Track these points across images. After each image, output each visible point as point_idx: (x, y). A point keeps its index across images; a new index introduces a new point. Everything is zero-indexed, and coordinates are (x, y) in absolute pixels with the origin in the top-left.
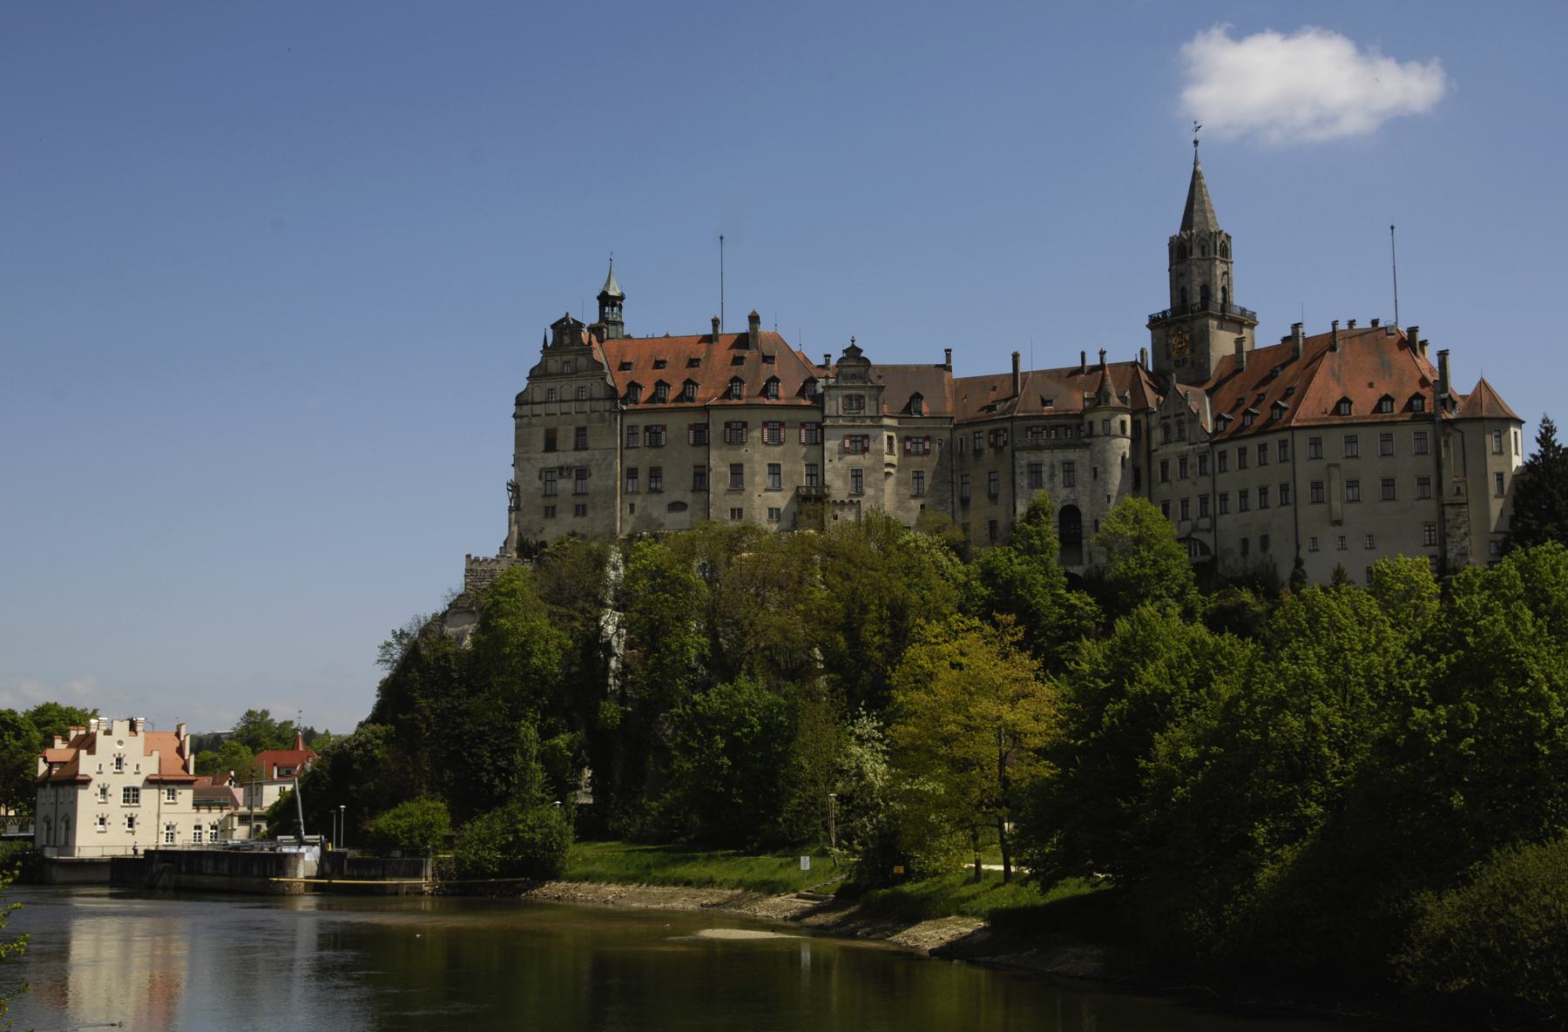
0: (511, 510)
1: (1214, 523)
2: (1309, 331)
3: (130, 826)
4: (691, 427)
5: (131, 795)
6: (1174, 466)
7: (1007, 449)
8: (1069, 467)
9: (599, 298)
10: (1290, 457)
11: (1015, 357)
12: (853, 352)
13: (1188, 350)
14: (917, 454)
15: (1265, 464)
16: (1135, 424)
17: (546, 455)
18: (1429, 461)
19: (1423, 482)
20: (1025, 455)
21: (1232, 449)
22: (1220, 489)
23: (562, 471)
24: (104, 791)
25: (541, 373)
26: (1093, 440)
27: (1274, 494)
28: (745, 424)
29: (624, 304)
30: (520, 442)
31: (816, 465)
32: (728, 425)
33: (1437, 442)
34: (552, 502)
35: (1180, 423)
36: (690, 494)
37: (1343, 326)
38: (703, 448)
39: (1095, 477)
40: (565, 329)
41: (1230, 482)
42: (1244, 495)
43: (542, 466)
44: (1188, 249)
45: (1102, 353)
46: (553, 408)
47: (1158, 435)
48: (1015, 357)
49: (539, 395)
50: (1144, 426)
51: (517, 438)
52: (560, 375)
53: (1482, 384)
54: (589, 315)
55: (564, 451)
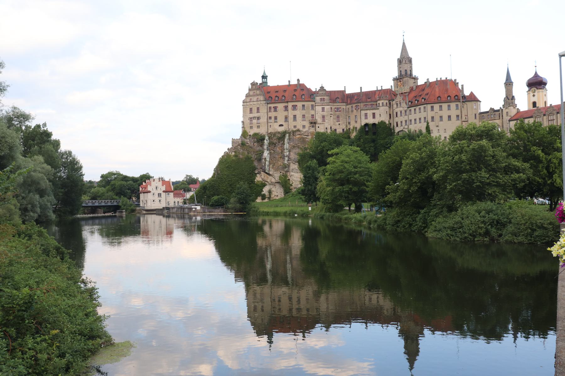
0: (242, 127)
2: (431, 81)
3: (160, 202)
4: (284, 107)
5: (159, 195)
7: (359, 110)
8: (374, 114)
10: (426, 110)
11: (361, 88)
12: (322, 88)
16: (390, 103)
19: (458, 116)
20: (363, 111)
21: (412, 109)
24: (154, 194)
27: (423, 120)
28: (297, 106)
29: (268, 78)
32: (292, 106)
33: (461, 106)
34: (251, 125)
35: (400, 103)
39: (380, 116)
40: (253, 84)
41: (412, 117)
42: (415, 120)
45: (382, 86)
46: (251, 103)
47: (395, 106)
48: (361, 88)
49: (248, 100)
50: (392, 104)
51: (243, 110)
53: (472, 94)
54: (259, 81)
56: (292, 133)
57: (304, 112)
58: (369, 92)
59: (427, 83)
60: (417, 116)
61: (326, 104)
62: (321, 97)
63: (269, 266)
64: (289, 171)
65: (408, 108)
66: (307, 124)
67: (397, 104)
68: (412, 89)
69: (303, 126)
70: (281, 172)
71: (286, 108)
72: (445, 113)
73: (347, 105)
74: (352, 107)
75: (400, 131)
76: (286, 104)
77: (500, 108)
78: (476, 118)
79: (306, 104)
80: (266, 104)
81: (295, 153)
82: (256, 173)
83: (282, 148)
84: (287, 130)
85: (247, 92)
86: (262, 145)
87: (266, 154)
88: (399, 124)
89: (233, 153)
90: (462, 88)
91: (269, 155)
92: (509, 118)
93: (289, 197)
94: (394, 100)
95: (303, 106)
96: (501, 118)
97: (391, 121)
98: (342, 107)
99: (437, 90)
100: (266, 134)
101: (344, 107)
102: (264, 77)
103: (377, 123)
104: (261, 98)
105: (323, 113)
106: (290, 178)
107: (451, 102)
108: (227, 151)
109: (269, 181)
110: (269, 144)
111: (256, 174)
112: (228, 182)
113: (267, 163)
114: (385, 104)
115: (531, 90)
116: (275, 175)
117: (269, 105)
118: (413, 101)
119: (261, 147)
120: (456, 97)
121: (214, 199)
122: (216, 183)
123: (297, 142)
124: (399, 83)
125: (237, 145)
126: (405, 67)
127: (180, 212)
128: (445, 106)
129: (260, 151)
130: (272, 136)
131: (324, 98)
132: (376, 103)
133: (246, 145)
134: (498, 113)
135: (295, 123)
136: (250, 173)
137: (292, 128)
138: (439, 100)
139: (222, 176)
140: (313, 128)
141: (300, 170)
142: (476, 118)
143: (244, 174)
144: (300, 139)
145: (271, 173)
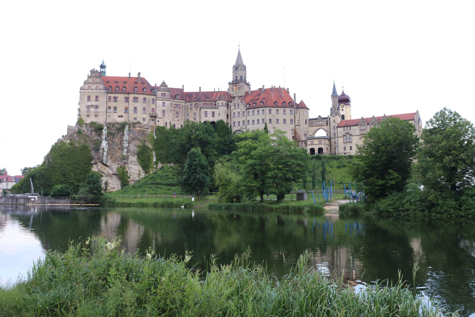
0: (78, 115)
1: (246, 127)
2: (266, 87)
4: (124, 98)
6: (237, 114)
7: (199, 108)
8: (213, 113)
9: (100, 66)
10: (265, 113)
11: (200, 88)
12: (164, 83)
13: (237, 90)
14: (177, 108)
15: (254, 115)
16: (228, 104)
17: (88, 102)
19: (291, 120)
20: (204, 109)
21: (251, 111)
22: (248, 120)
25: (87, 82)
27: (261, 121)
28: (138, 98)
29: (106, 68)
30: (81, 98)
31: (154, 109)
32: (134, 98)
34: (88, 114)
35: (238, 105)
37: (273, 87)
39: (219, 116)
41: (250, 118)
43: (86, 105)
46: (90, 91)
48: (200, 88)
49: (86, 87)
50: (229, 105)
52: (93, 83)
53: (302, 102)
54: (99, 69)
56: (132, 124)
57: (145, 105)
58: (207, 92)
59: (263, 89)
60: (256, 117)
61: (167, 99)
62: (162, 92)
64: (127, 163)
65: (246, 109)
66: (147, 117)
67: (235, 105)
68: (247, 93)
69: (143, 118)
70: (119, 164)
71: (127, 99)
72: (281, 116)
73: (186, 102)
75: (237, 130)
76: (127, 96)
77: (328, 116)
78: (306, 123)
79: (147, 97)
80: (105, 93)
81: (135, 145)
82: (93, 163)
84: (127, 121)
85: (86, 78)
86: (100, 135)
87: (104, 144)
88: (237, 124)
89: (68, 141)
90: (295, 97)
91: (107, 146)
92: (336, 125)
93: (130, 190)
94: (232, 102)
95: (145, 99)
96: (329, 124)
97: (229, 121)
98: (182, 104)
99: (273, 96)
100: (105, 124)
101: (184, 104)
102: (102, 67)
103: (216, 121)
104: (101, 86)
105: (163, 107)
106: (128, 170)
107: (286, 107)
108: (62, 138)
109: (105, 172)
110: (107, 134)
111: (92, 164)
112: (61, 172)
113: (105, 154)
114: (224, 104)
115: (340, 105)
116: (113, 166)
117: (109, 95)
118: (251, 103)
119: (99, 136)
120: (290, 104)
121: (56, 188)
122: (47, 172)
123: (137, 134)
124: (235, 87)
125: (73, 132)
126: (240, 73)
127: (11, 203)
128: (281, 110)
129: (98, 140)
130: (111, 126)
132: (215, 103)
133: (82, 134)
134: (326, 120)
135: (135, 116)
136: (87, 163)
137: (132, 120)
138: (275, 105)
139: (54, 164)
140: (153, 122)
141: (139, 162)
142: (306, 123)
143: (80, 164)
144: (140, 131)
145: (108, 164)
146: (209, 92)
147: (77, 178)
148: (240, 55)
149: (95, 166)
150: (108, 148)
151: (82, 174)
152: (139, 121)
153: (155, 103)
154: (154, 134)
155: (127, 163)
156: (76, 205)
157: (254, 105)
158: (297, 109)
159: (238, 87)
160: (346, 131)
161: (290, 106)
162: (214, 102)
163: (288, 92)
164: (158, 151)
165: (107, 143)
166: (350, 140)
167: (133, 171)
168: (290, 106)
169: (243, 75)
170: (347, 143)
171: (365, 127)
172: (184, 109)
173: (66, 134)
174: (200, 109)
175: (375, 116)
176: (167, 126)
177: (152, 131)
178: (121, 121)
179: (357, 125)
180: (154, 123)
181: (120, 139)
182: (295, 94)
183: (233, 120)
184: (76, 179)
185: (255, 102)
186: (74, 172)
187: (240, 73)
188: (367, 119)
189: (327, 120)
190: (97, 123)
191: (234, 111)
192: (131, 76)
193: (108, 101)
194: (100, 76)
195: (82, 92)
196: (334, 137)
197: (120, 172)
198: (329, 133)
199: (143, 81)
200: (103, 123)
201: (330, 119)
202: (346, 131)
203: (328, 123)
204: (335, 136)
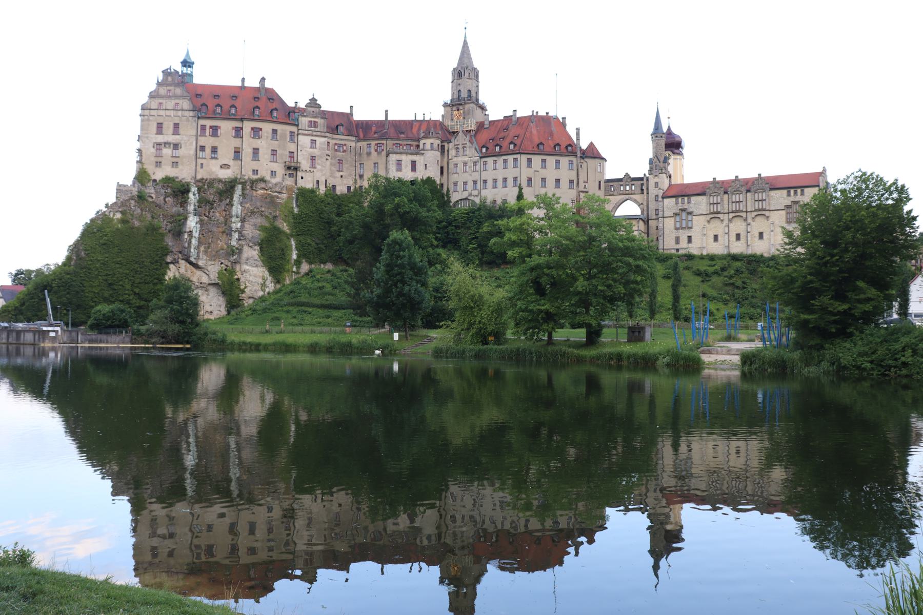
0: (137, 162)
4: (233, 128)
6: (461, 166)
7: (384, 153)
8: (414, 164)
11: (387, 111)
12: (313, 102)
14: (340, 151)
18: (574, 173)
19: (571, 181)
20: (394, 155)
21: (490, 160)
22: (483, 178)
23: (166, 144)
25: (156, 94)
26: (425, 152)
27: (510, 182)
29: (194, 66)
30: (143, 128)
32: (252, 129)
34: (159, 159)
36: (232, 161)
37: (535, 114)
38: (240, 140)
39: (426, 169)
43: (155, 141)
44: (463, 73)
46: (162, 113)
48: (387, 111)
49: (154, 105)
53: (591, 146)
54: (179, 68)
55: (167, 135)
56: (248, 183)
57: (275, 144)
58: (399, 121)
60: (500, 174)
61: (319, 134)
63: (190, 461)
64: (239, 262)
66: (280, 169)
67: (457, 149)
68: (481, 126)
69: (272, 172)
70: (222, 263)
71: (238, 132)
73: (359, 140)
74: (369, 146)
76: (238, 124)
77: (645, 175)
78: (600, 188)
79: (279, 127)
80: (194, 119)
81: (255, 225)
82: (169, 261)
83: (228, 213)
84: (239, 177)
85: (153, 87)
86: (184, 203)
87: (192, 223)
88: (460, 186)
89: (119, 216)
90: (578, 134)
91: (199, 226)
92: (661, 193)
93: (247, 316)
94: (451, 142)
95: (275, 131)
96: (645, 191)
97: (444, 181)
98: (349, 144)
99: (534, 132)
100: (193, 181)
101: (353, 144)
102: (187, 63)
104: (186, 104)
106: (240, 276)
107: (561, 155)
108: (105, 209)
110: (199, 202)
111: (168, 263)
112: (105, 278)
113: (194, 242)
114: (435, 146)
116: (209, 268)
117: (202, 122)
118: (490, 146)
119: (181, 206)
120: (569, 148)
121: (100, 311)
122: (74, 278)
124: (455, 113)
125: (127, 198)
126: (466, 84)
127: (4, 341)
128: (551, 160)
129: (179, 215)
130: (206, 187)
131: (317, 122)
132: (417, 143)
133: (147, 200)
135: (255, 165)
136: (157, 261)
137: (248, 174)
138: (539, 149)
139: (90, 263)
140: (291, 179)
141: (262, 261)
142: (600, 188)
143: (143, 262)
144: (264, 197)
145: (201, 263)
146: (405, 122)
147: (137, 290)
148: (468, 47)
149: (174, 267)
150: (200, 231)
151: (148, 283)
152: (264, 177)
153: (296, 142)
154: (292, 204)
155: (239, 262)
156: (143, 345)
157: (497, 149)
158: (583, 158)
159: (464, 113)
160: (680, 204)
161: (570, 152)
162: (415, 140)
163: (563, 125)
164: (301, 238)
165: (198, 220)
166: (687, 224)
167: (251, 279)
168: (570, 152)
169: (473, 89)
170: (682, 228)
171: (719, 197)
172: (353, 153)
173: (114, 200)
174: (387, 156)
175: (739, 178)
176: (320, 187)
177: (290, 198)
178: (226, 177)
179: (703, 194)
180: (294, 182)
181: (224, 213)
182: (578, 129)
183: (454, 178)
184: (135, 294)
185: (498, 142)
186: (130, 278)
187: (466, 84)
188: (723, 182)
189: (642, 182)
190: (177, 180)
191: (456, 160)
192: (246, 85)
193: (199, 134)
194: (182, 82)
195: (145, 114)
196: (654, 217)
197: (225, 279)
198: (645, 208)
199: (272, 96)
200: (188, 180)
201: (647, 180)
202: (680, 206)
203: (644, 188)
204: (657, 215)
